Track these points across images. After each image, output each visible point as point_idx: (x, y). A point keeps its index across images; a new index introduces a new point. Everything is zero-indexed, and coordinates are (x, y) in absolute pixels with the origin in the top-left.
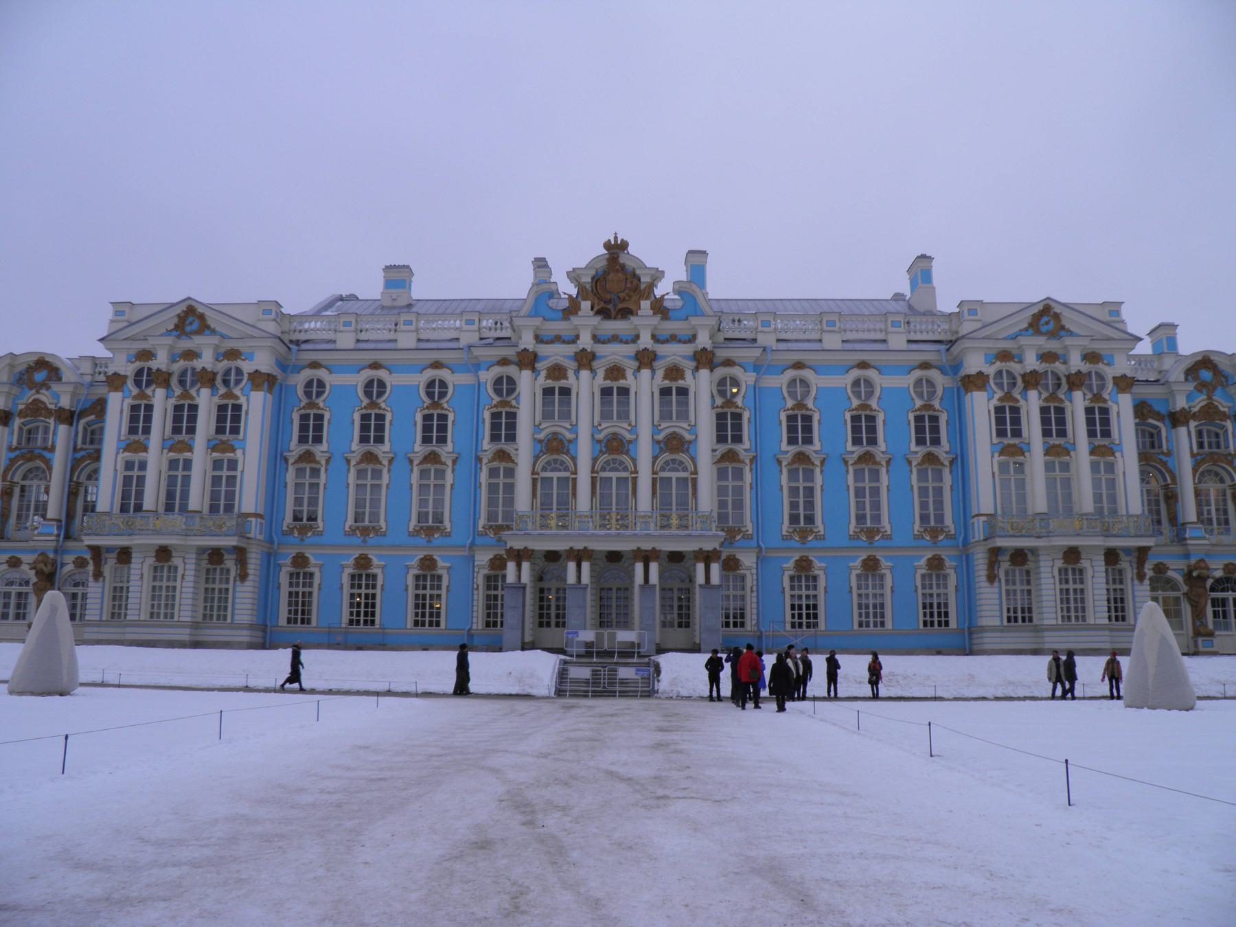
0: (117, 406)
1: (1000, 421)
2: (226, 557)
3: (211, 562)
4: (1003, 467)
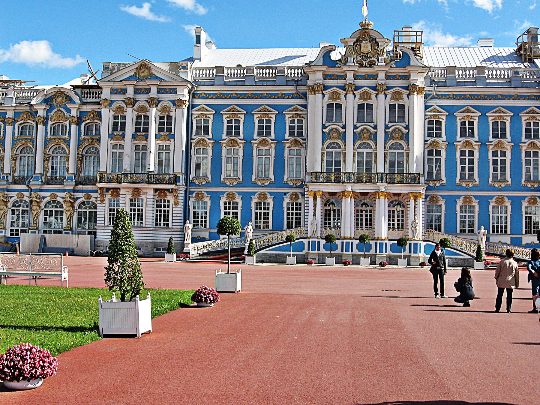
2: (168, 194)
3: (159, 195)
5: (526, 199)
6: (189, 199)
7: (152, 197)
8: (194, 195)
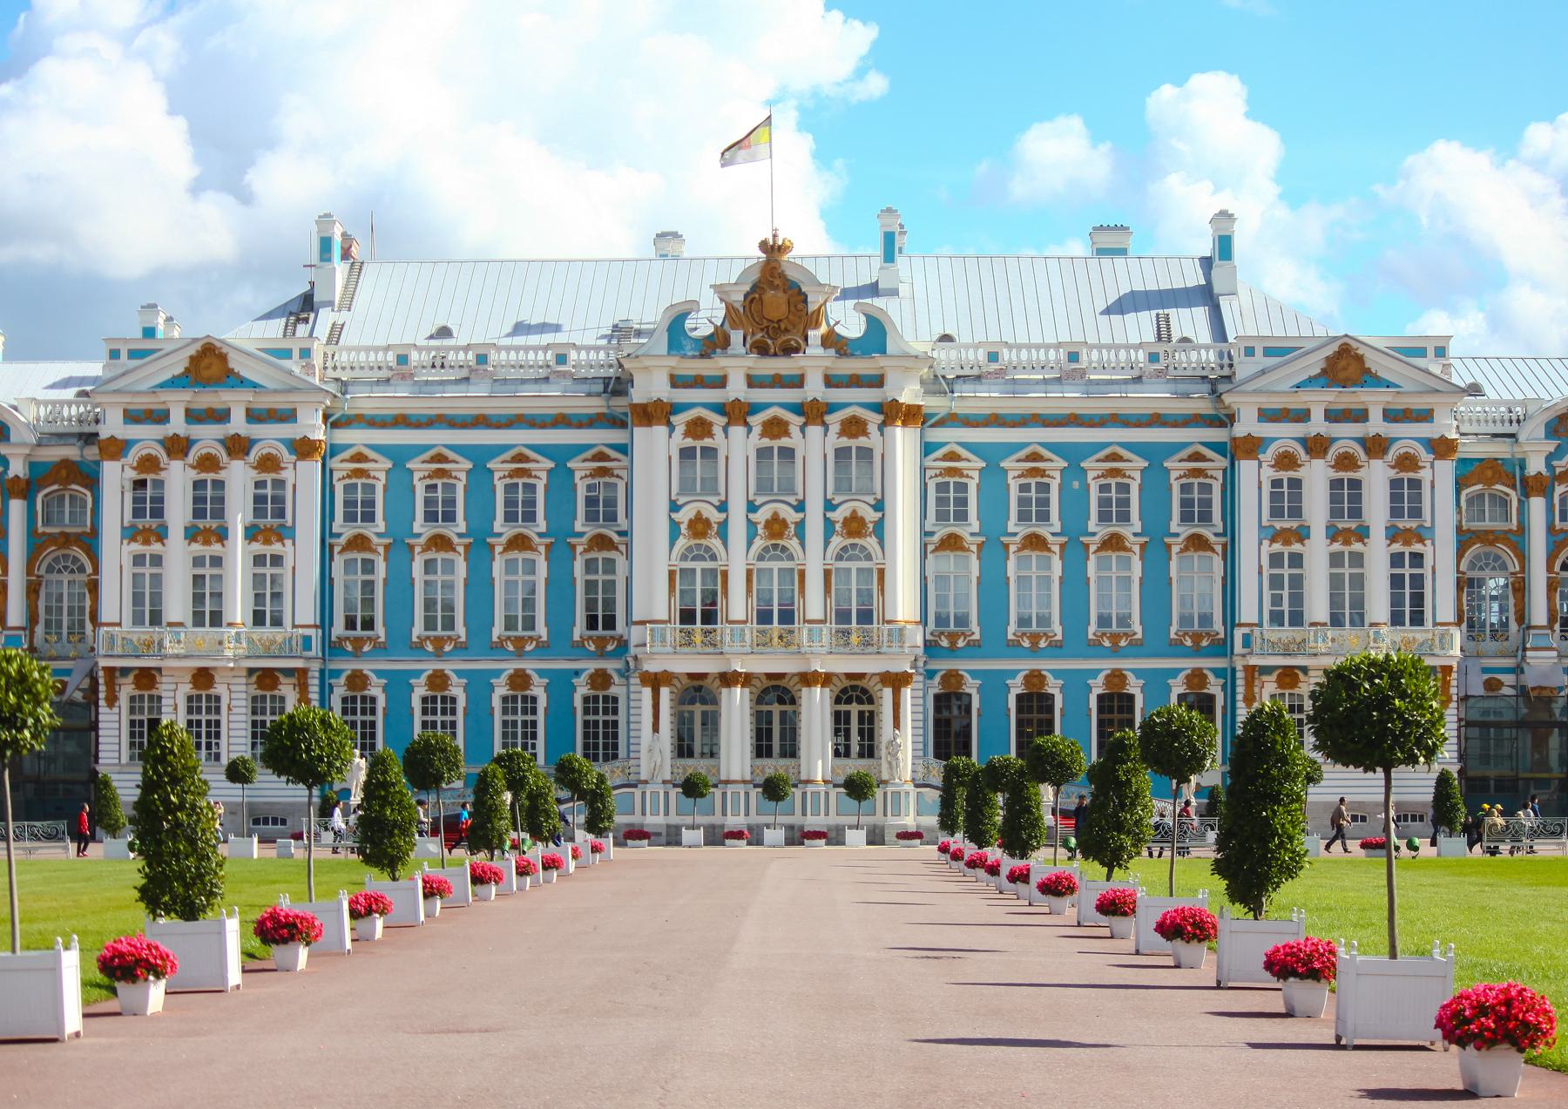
0: (115, 477)
1: (1276, 497)
2: (282, 679)
3: (261, 684)
4: (1276, 560)
5: (1181, 676)
6: (331, 691)
7: (243, 688)
8: (342, 680)
